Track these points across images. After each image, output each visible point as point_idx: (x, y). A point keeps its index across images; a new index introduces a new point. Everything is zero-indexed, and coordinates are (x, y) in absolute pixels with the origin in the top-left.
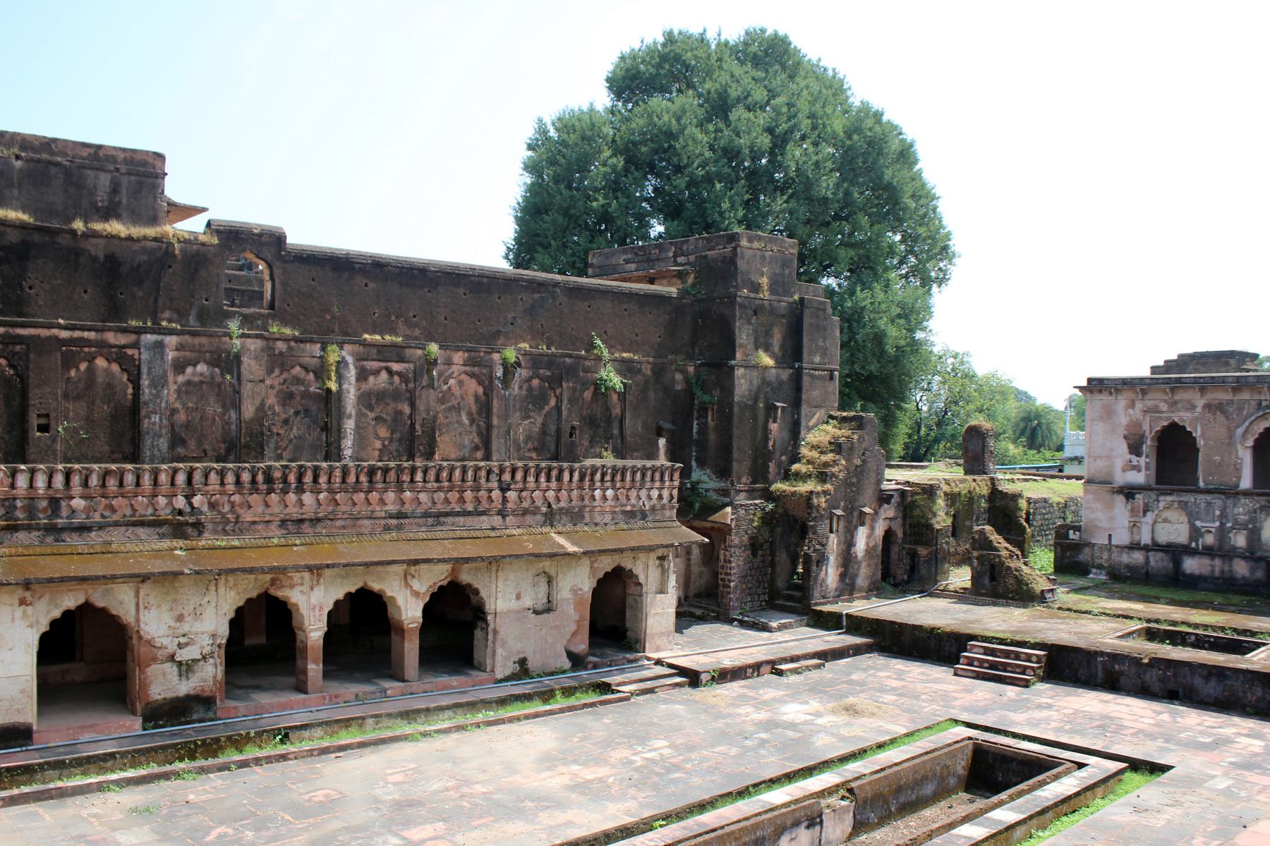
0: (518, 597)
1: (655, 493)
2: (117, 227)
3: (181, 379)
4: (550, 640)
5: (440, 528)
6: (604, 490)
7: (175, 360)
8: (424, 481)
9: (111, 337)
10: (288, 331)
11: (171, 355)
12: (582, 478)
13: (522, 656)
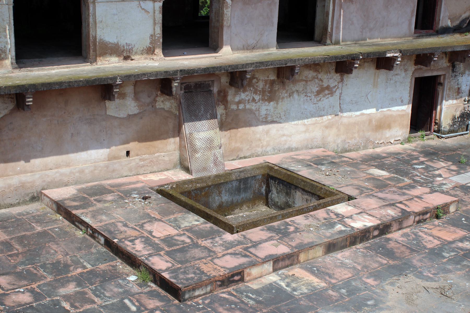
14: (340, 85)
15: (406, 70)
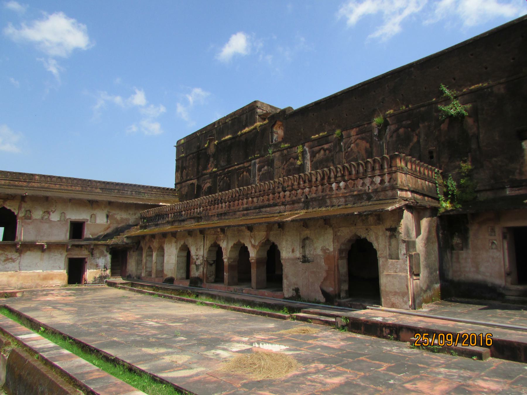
0: (293, 251)
1: (378, 179)
2: (247, 130)
3: (261, 173)
4: (311, 280)
5: (260, 214)
6: (338, 183)
7: (259, 167)
8: (255, 192)
9: (246, 165)
10: (286, 145)
11: (257, 166)
12: (323, 179)
13: (296, 287)
14: (19, 258)
15: (61, 254)
